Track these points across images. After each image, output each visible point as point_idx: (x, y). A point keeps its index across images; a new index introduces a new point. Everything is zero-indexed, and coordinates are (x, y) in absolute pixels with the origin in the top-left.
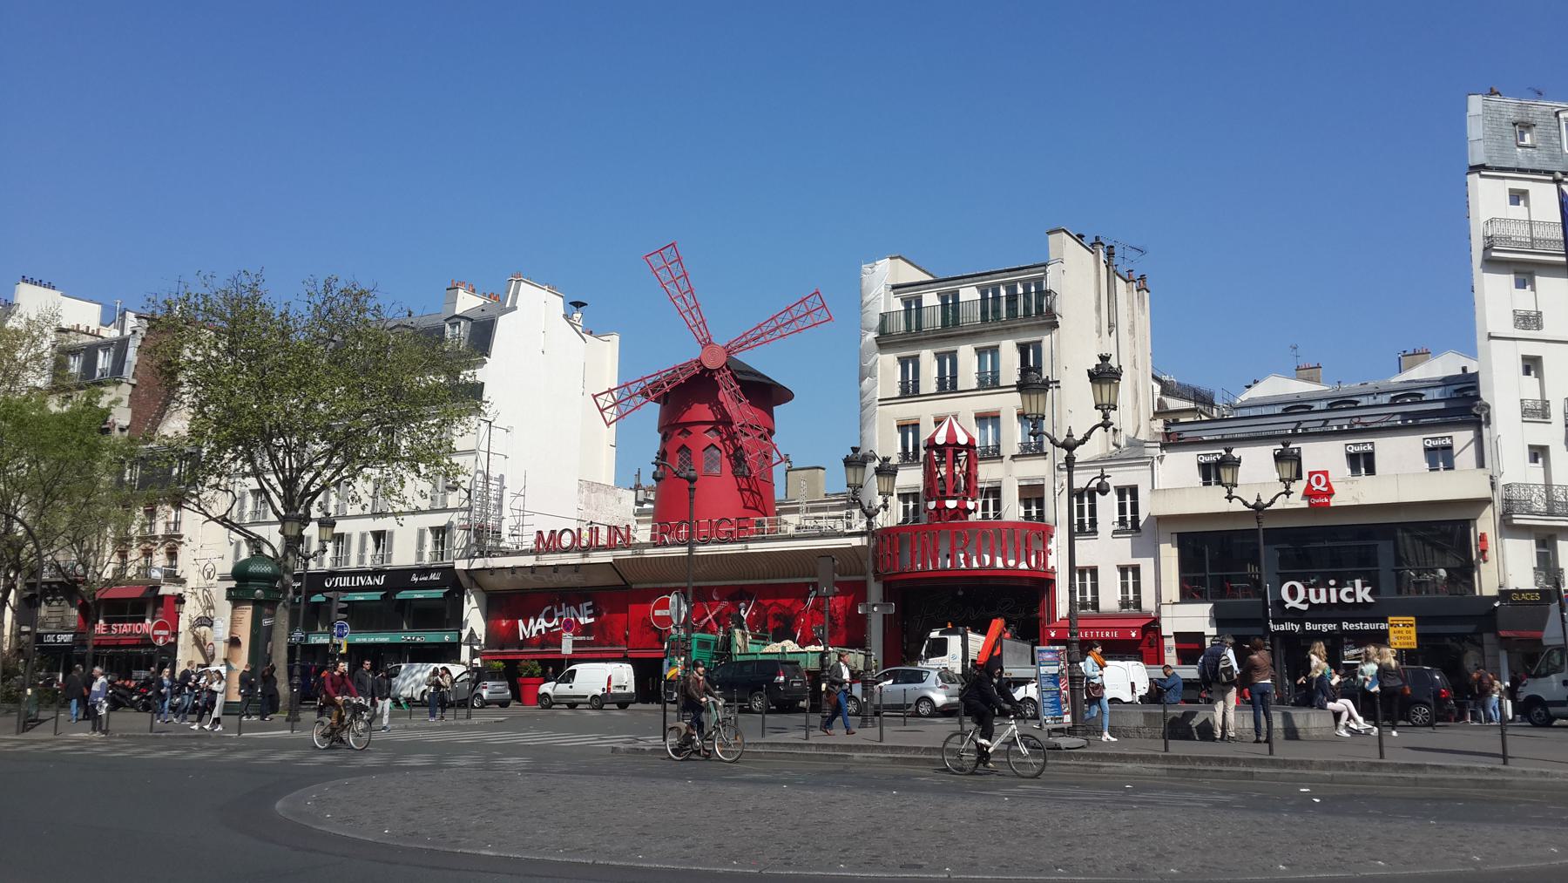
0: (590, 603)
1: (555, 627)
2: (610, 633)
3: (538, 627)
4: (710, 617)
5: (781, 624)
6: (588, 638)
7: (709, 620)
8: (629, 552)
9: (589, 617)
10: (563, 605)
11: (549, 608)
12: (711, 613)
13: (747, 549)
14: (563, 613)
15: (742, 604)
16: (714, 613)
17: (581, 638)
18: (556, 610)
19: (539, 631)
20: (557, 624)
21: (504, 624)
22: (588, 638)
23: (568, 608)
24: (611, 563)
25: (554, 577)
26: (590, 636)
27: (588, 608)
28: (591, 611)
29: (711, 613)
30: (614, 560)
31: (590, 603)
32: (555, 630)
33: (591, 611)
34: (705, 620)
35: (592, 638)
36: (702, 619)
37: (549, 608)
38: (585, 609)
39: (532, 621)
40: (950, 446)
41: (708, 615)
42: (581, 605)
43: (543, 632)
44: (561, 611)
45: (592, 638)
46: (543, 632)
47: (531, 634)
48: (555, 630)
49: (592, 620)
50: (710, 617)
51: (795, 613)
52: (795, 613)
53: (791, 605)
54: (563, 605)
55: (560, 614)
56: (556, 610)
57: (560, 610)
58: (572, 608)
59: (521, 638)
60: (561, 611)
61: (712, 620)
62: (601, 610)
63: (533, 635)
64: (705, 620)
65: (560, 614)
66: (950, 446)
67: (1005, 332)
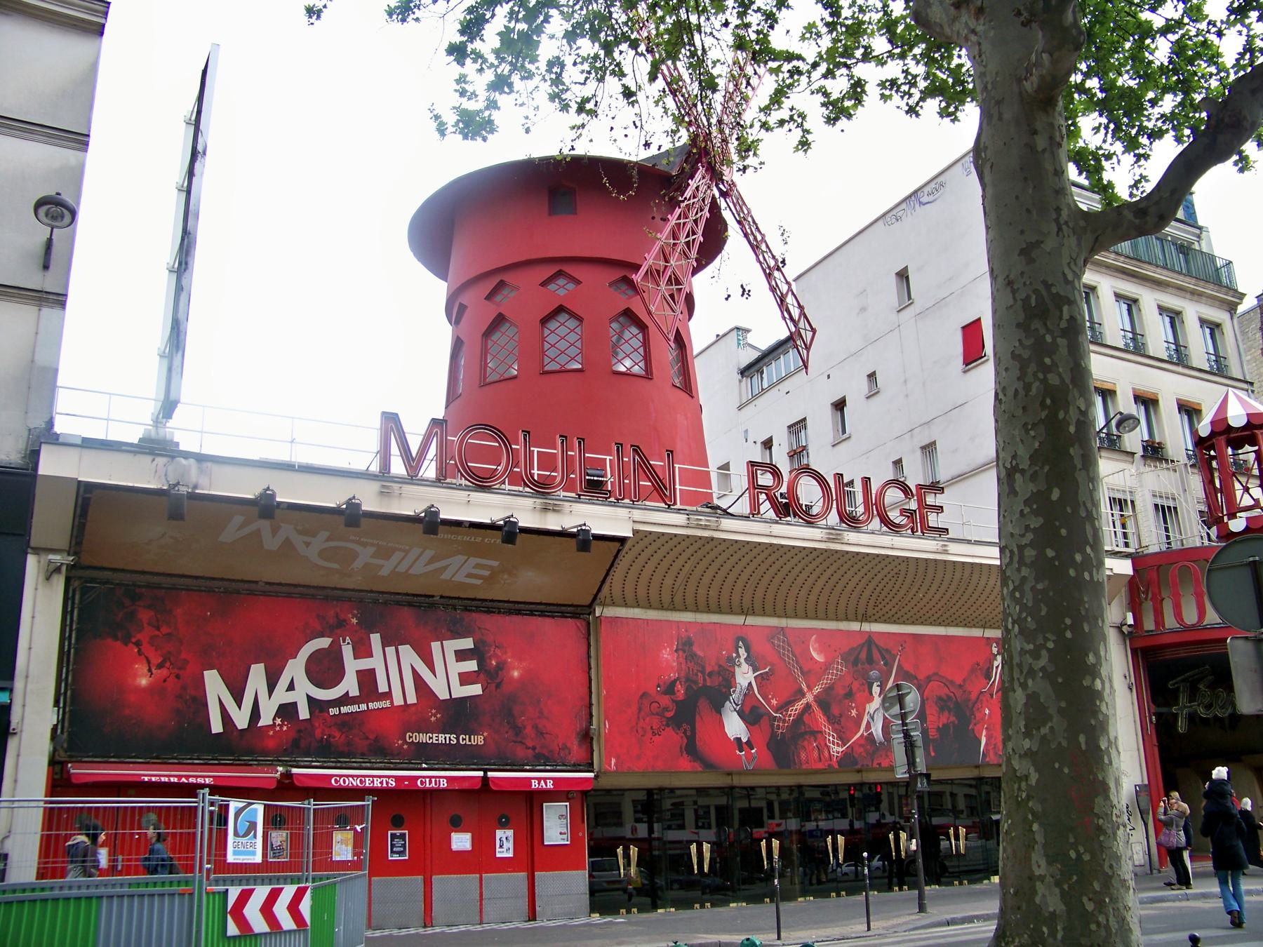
0: (467, 643)
1: (345, 699)
2: (536, 727)
3: (282, 696)
4: (809, 698)
5: (953, 719)
6: (464, 740)
7: (808, 706)
8: (680, 519)
9: (465, 679)
10: (375, 639)
11: (324, 643)
12: (810, 688)
13: (946, 552)
14: (375, 662)
15: (874, 673)
16: (817, 690)
17: (442, 738)
18: (347, 651)
19: (287, 711)
20: (355, 692)
21: (144, 682)
22: (464, 740)
23: (390, 650)
24: (622, 540)
25: (397, 556)
26: (470, 733)
27: (461, 655)
28: (472, 666)
29: (810, 689)
30: (635, 532)
31: (467, 643)
32: (344, 710)
33: (472, 666)
34: (799, 706)
35: (478, 740)
36: (791, 703)
37: (324, 643)
38: (451, 657)
39: (257, 675)
40: (1220, 434)
41: (803, 695)
42: (435, 646)
43: (304, 713)
44: (369, 654)
45: (478, 740)
46: (304, 713)
47: (255, 713)
48: (344, 710)
49: (476, 690)
50: (809, 698)
51: (974, 696)
52: (974, 696)
53: (964, 680)
54: (375, 639)
55: (365, 664)
56: (347, 651)
57: (363, 651)
58: (407, 651)
59: (217, 727)
60: (369, 654)
61: (815, 708)
62: (501, 666)
63: (266, 720)
64: (799, 706)
65: (365, 664)
66: (1220, 434)
67: (1188, 296)
